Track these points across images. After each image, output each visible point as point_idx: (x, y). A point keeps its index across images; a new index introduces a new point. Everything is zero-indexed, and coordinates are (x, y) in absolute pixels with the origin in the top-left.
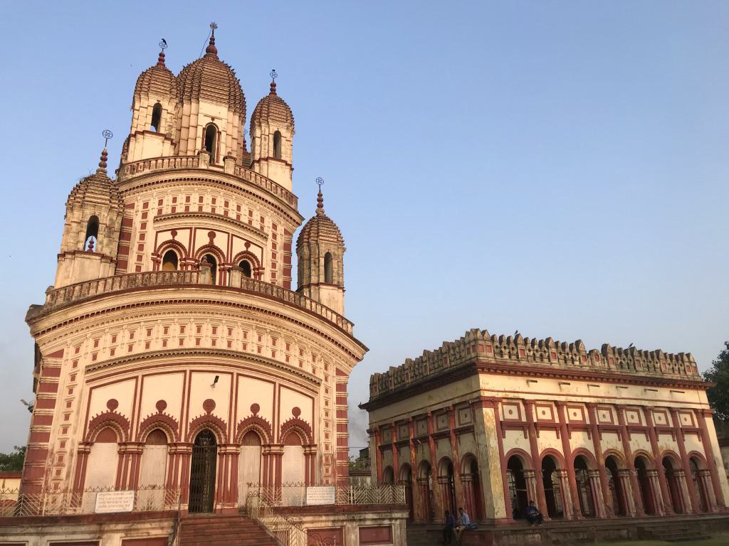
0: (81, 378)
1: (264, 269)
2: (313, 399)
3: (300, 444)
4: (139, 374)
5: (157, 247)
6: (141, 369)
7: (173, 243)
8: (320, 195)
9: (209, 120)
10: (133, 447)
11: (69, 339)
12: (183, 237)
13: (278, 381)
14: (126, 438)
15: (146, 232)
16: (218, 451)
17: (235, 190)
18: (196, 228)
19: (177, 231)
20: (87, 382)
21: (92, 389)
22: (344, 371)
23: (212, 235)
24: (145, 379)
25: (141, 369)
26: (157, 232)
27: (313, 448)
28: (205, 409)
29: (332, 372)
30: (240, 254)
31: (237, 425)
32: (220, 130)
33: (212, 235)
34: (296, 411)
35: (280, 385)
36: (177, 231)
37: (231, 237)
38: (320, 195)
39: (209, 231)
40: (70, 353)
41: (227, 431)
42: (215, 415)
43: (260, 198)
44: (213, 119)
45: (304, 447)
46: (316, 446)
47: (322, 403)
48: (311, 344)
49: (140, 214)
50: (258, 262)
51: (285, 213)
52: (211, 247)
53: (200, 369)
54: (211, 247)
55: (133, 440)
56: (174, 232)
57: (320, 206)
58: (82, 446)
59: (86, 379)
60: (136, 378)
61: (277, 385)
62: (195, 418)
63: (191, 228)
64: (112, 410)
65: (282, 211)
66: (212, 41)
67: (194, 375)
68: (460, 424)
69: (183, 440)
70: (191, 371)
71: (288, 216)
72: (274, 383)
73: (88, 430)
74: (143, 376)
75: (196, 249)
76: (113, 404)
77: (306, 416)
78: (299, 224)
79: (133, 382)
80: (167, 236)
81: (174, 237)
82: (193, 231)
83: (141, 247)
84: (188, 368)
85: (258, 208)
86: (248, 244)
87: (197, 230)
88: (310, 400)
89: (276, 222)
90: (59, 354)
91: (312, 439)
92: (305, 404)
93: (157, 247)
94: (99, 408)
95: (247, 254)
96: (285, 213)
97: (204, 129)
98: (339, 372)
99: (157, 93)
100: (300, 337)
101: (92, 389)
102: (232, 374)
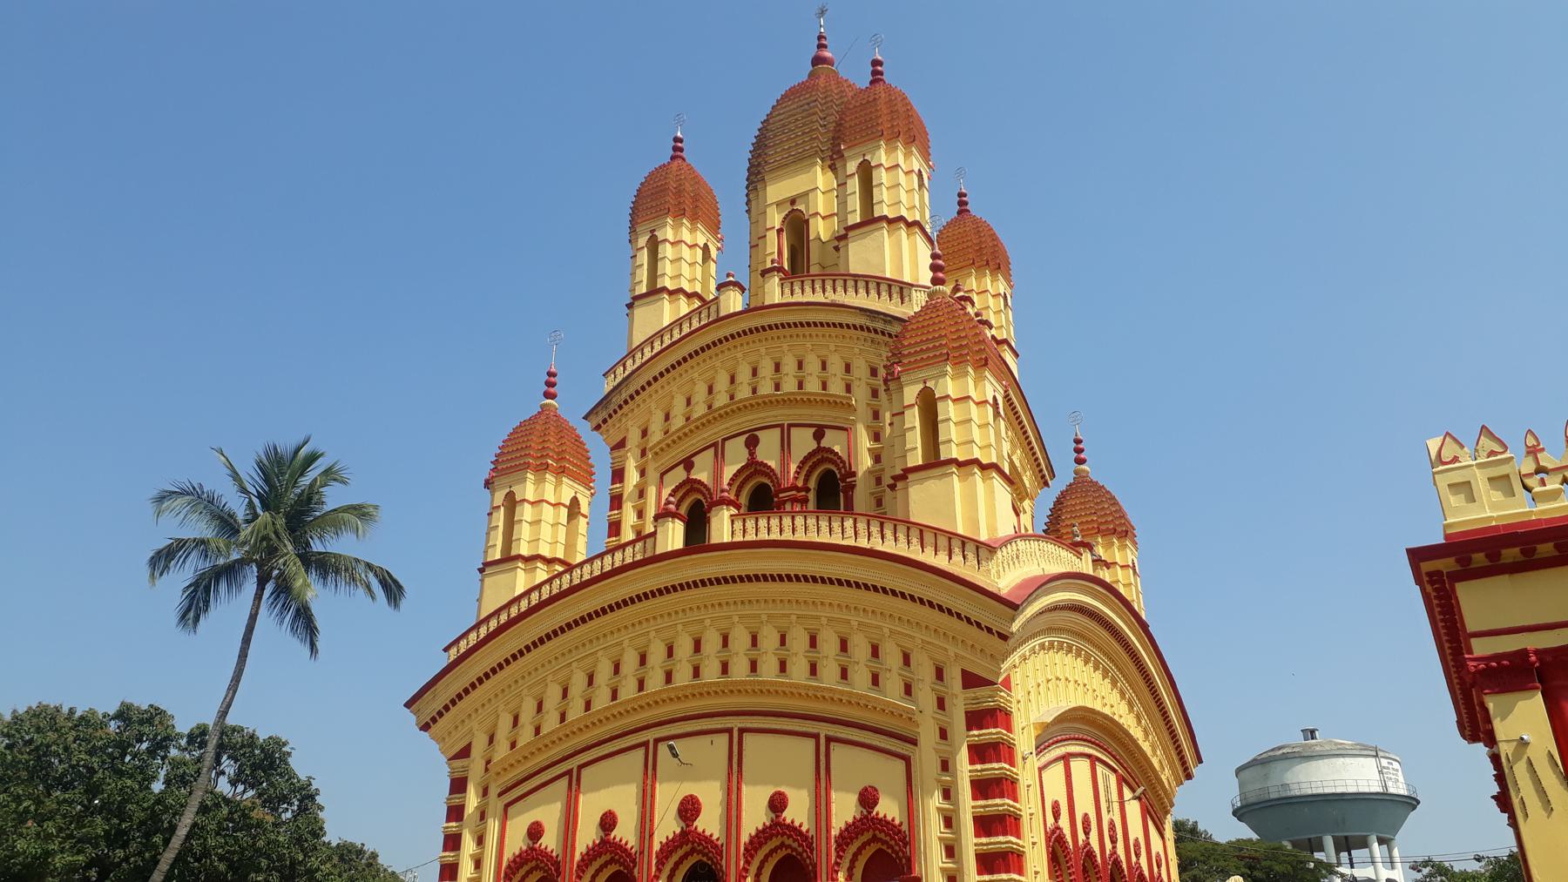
2: (907, 760)
4: (573, 764)
18: (724, 440)
20: (500, 795)
24: (585, 773)
26: (662, 475)
30: (806, 459)
33: (752, 442)
35: (829, 740)
37: (785, 431)
48: (887, 626)
54: (754, 467)
56: (688, 464)
61: (823, 741)
62: (664, 841)
63: (715, 445)
65: (876, 331)
74: (581, 767)
76: (535, 832)
82: (718, 448)
85: (832, 348)
86: (819, 434)
88: (900, 765)
92: (885, 773)
94: (516, 842)
95: (821, 455)
97: (780, 231)
98: (971, 680)
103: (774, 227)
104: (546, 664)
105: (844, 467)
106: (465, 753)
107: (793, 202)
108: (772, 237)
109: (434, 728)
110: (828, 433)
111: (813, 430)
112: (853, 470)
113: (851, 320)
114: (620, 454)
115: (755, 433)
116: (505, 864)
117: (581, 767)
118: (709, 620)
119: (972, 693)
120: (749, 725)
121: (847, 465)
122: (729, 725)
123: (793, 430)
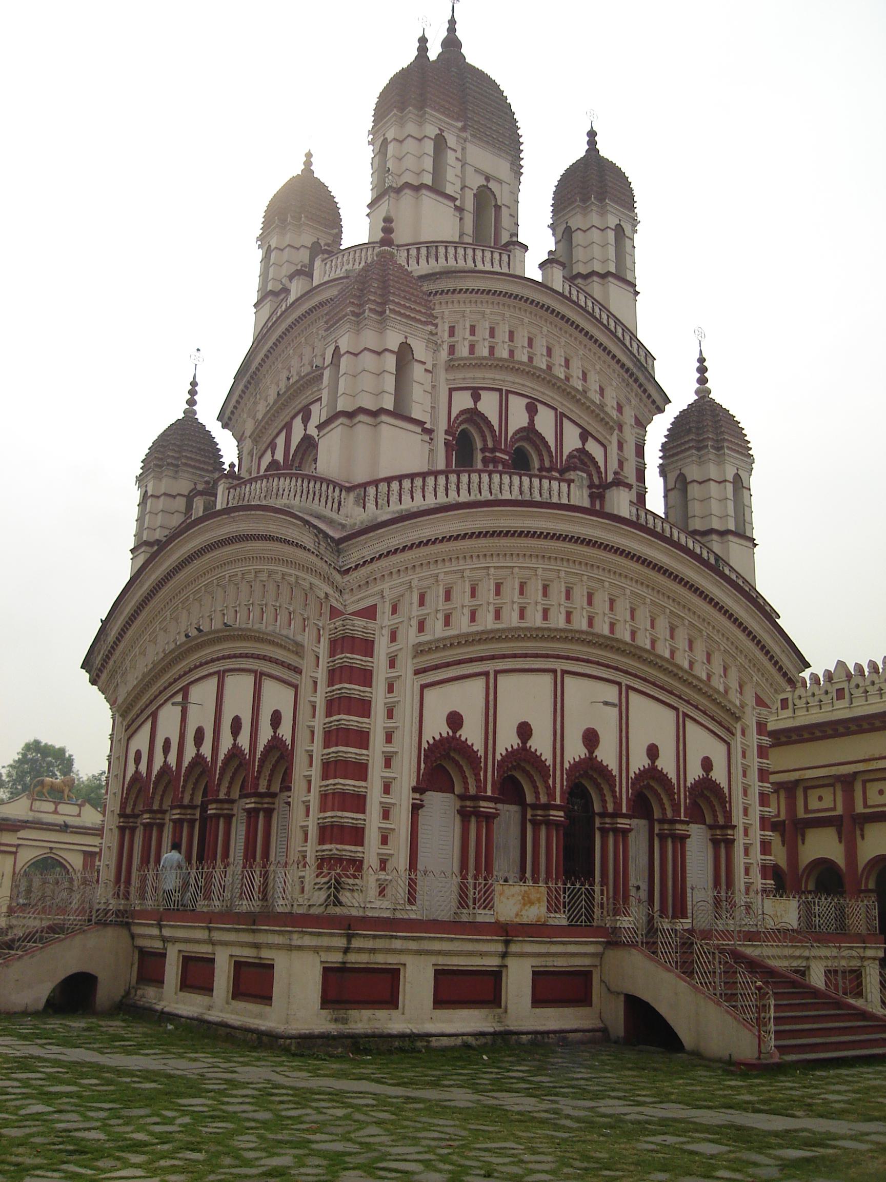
0: (407, 666)
2: (728, 744)
3: (704, 823)
5: (452, 420)
6: (493, 658)
7: (474, 416)
8: (702, 360)
9: (483, 182)
12: (489, 405)
13: (684, 708)
16: (597, 825)
17: (567, 327)
19: (481, 392)
20: (417, 672)
21: (423, 687)
23: (532, 410)
25: (493, 658)
26: (451, 390)
28: (586, 746)
29: (750, 700)
31: (630, 780)
32: (499, 204)
34: (707, 764)
36: (481, 392)
37: (560, 418)
38: (702, 360)
39: (529, 400)
40: (385, 618)
41: (617, 789)
43: (605, 349)
44: (488, 179)
45: (711, 827)
46: (734, 827)
50: (599, 473)
51: (640, 386)
52: (530, 433)
54: (530, 433)
56: (476, 398)
57: (703, 381)
60: (486, 674)
63: (500, 390)
64: (454, 732)
65: (636, 380)
68: (866, 805)
71: (645, 391)
72: (676, 709)
73: (423, 766)
75: (510, 435)
77: (719, 775)
78: (661, 410)
79: (480, 683)
80: (463, 401)
81: (475, 403)
84: (559, 665)
85: (598, 367)
86: (585, 435)
89: (623, 401)
90: (370, 613)
91: (728, 815)
94: (436, 728)
96: (640, 386)
101: (423, 687)
113: (624, 359)
115: (537, 403)
116: (425, 745)
118: (586, 577)
119: (759, 709)
121: (603, 475)
122: (618, 680)
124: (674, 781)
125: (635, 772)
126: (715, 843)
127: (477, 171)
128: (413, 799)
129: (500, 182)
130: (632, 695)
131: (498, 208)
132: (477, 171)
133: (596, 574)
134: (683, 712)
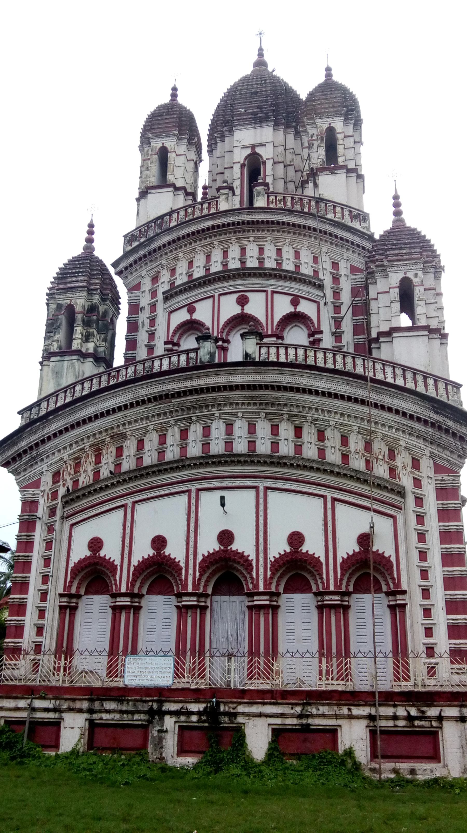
1: (321, 332)
4: (129, 501)
9: (249, 151)
10: (122, 599)
11: (44, 467)
14: (116, 590)
15: (156, 315)
19: (194, 305)
22: (447, 465)
23: (242, 301)
24: (139, 508)
27: (398, 597)
32: (265, 159)
33: (242, 301)
35: (334, 500)
42: (234, 549)
46: (404, 592)
47: (413, 519)
49: (148, 295)
53: (211, 485)
55: (123, 590)
56: (191, 310)
58: (65, 599)
59: (65, 515)
63: (213, 297)
66: (261, 54)
67: (202, 495)
69: (190, 589)
70: (199, 490)
79: (121, 512)
83: (152, 335)
84: (193, 487)
86: (295, 301)
87: (222, 298)
93: (170, 334)
97: (243, 166)
99: (158, 136)
100: (338, 419)
102: (256, 488)
103: (239, 162)
104: (115, 428)
105: (314, 326)
106: (36, 484)
107: (253, 147)
108: (237, 168)
109: (13, 466)
110: (302, 301)
111: (291, 297)
112: (321, 329)
114: (138, 294)
116: (71, 565)
117: (134, 503)
120: (274, 486)
122: (256, 484)
123: (275, 296)
124: (323, 560)
125: (274, 557)
126: (392, 608)
127: (243, 147)
128: (60, 602)
129: (262, 145)
130: (271, 495)
131: (264, 163)
132: (243, 147)
133: (228, 409)
134: (332, 497)
